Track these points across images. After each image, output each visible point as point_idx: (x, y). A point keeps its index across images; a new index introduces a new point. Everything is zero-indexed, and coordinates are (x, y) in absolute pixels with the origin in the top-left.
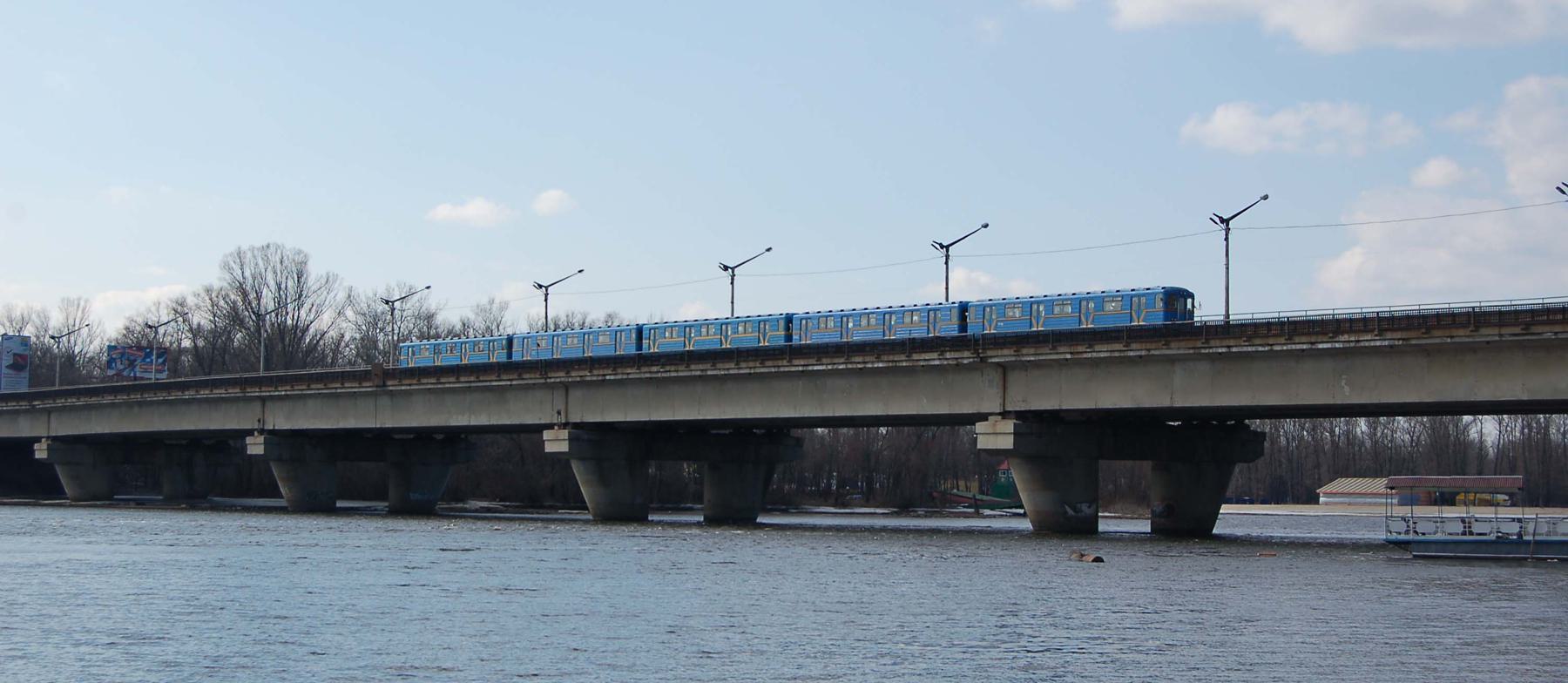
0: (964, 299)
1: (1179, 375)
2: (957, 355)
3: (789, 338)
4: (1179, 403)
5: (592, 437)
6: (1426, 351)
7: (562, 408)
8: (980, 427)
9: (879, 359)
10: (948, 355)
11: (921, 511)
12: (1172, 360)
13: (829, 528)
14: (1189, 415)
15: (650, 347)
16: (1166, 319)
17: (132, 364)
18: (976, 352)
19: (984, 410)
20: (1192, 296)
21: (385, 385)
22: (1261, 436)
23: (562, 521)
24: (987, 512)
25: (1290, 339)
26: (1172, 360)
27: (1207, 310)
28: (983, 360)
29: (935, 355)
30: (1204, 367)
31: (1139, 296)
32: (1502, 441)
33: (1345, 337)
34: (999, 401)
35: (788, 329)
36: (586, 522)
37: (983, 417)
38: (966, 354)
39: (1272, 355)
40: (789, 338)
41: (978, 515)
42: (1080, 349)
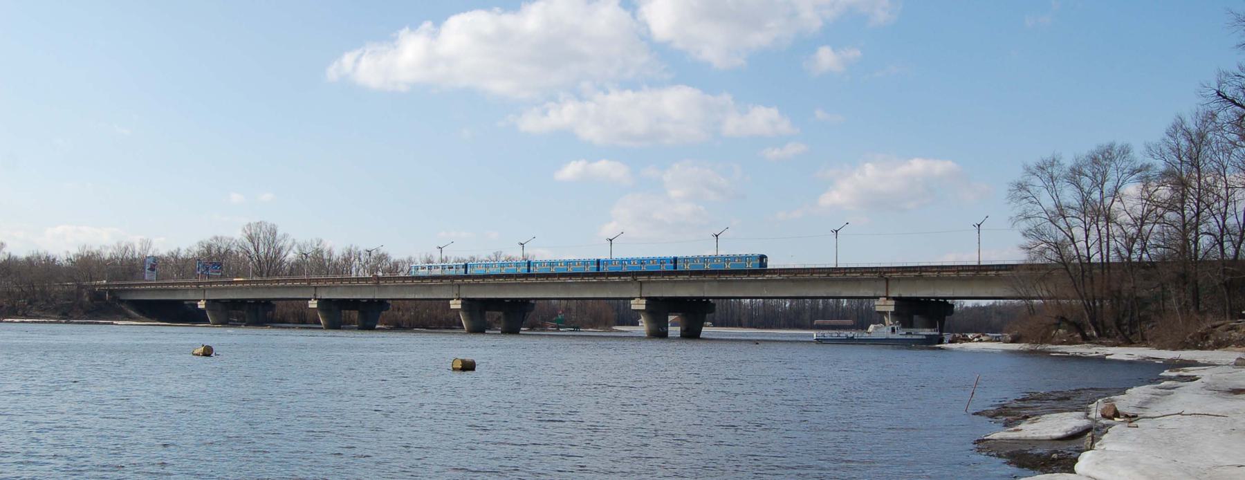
0: (676, 256)
1: (706, 286)
2: (626, 278)
3: (529, 270)
4: (705, 296)
5: (469, 304)
6: (793, 281)
7: (457, 292)
8: (632, 302)
9: (595, 279)
10: (622, 278)
11: (538, 329)
12: (704, 281)
13: (586, 336)
14: (512, 300)
15: (603, 269)
16: (760, 267)
17: (207, 269)
18: (633, 277)
19: (633, 296)
20: (766, 257)
21: (378, 283)
22: (275, 305)
23: (442, 333)
24: (562, 330)
25: (749, 276)
26: (704, 281)
27: (771, 264)
28: (635, 280)
29: (617, 278)
30: (715, 284)
31: (749, 257)
32: (729, 310)
33: (767, 276)
34: (639, 293)
35: (529, 266)
36: (465, 334)
37: (634, 299)
38: (629, 278)
39: (742, 281)
40: (529, 270)
41: (558, 330)
42: (673, 277)
